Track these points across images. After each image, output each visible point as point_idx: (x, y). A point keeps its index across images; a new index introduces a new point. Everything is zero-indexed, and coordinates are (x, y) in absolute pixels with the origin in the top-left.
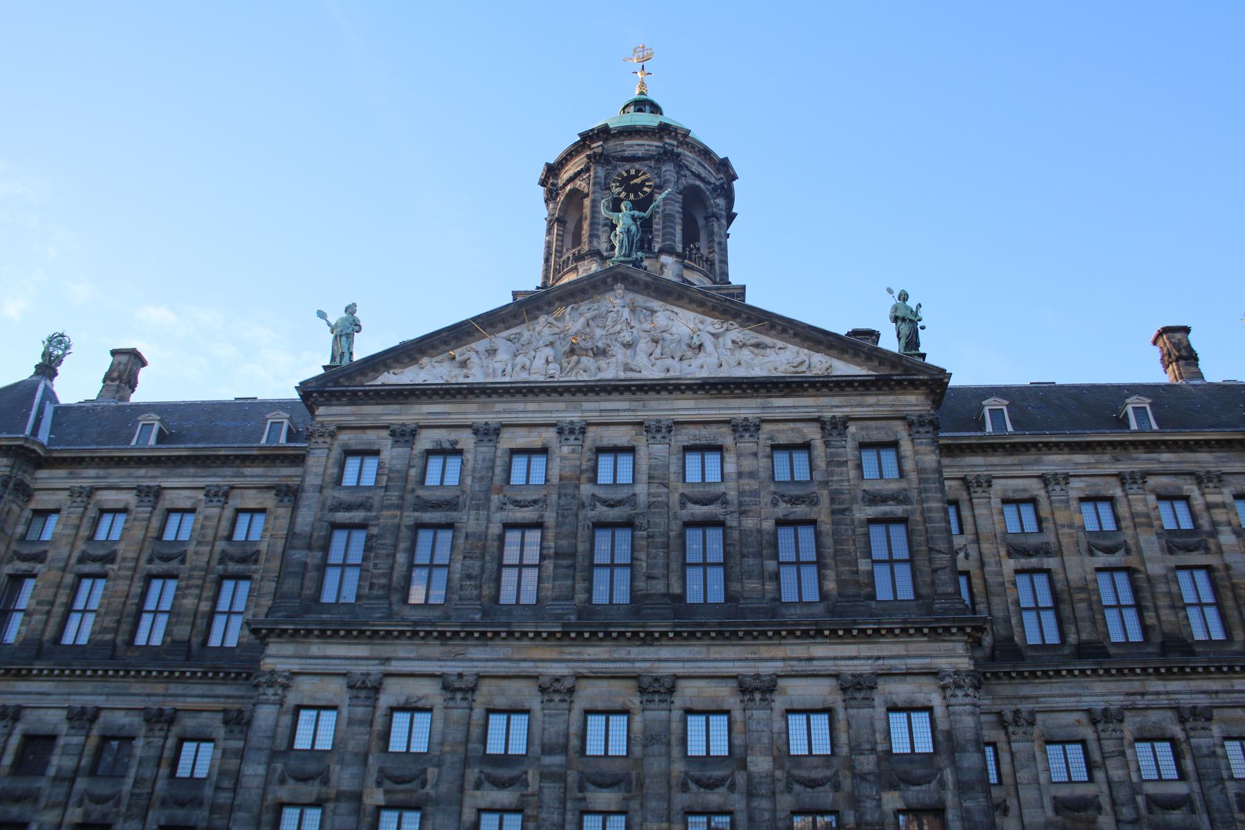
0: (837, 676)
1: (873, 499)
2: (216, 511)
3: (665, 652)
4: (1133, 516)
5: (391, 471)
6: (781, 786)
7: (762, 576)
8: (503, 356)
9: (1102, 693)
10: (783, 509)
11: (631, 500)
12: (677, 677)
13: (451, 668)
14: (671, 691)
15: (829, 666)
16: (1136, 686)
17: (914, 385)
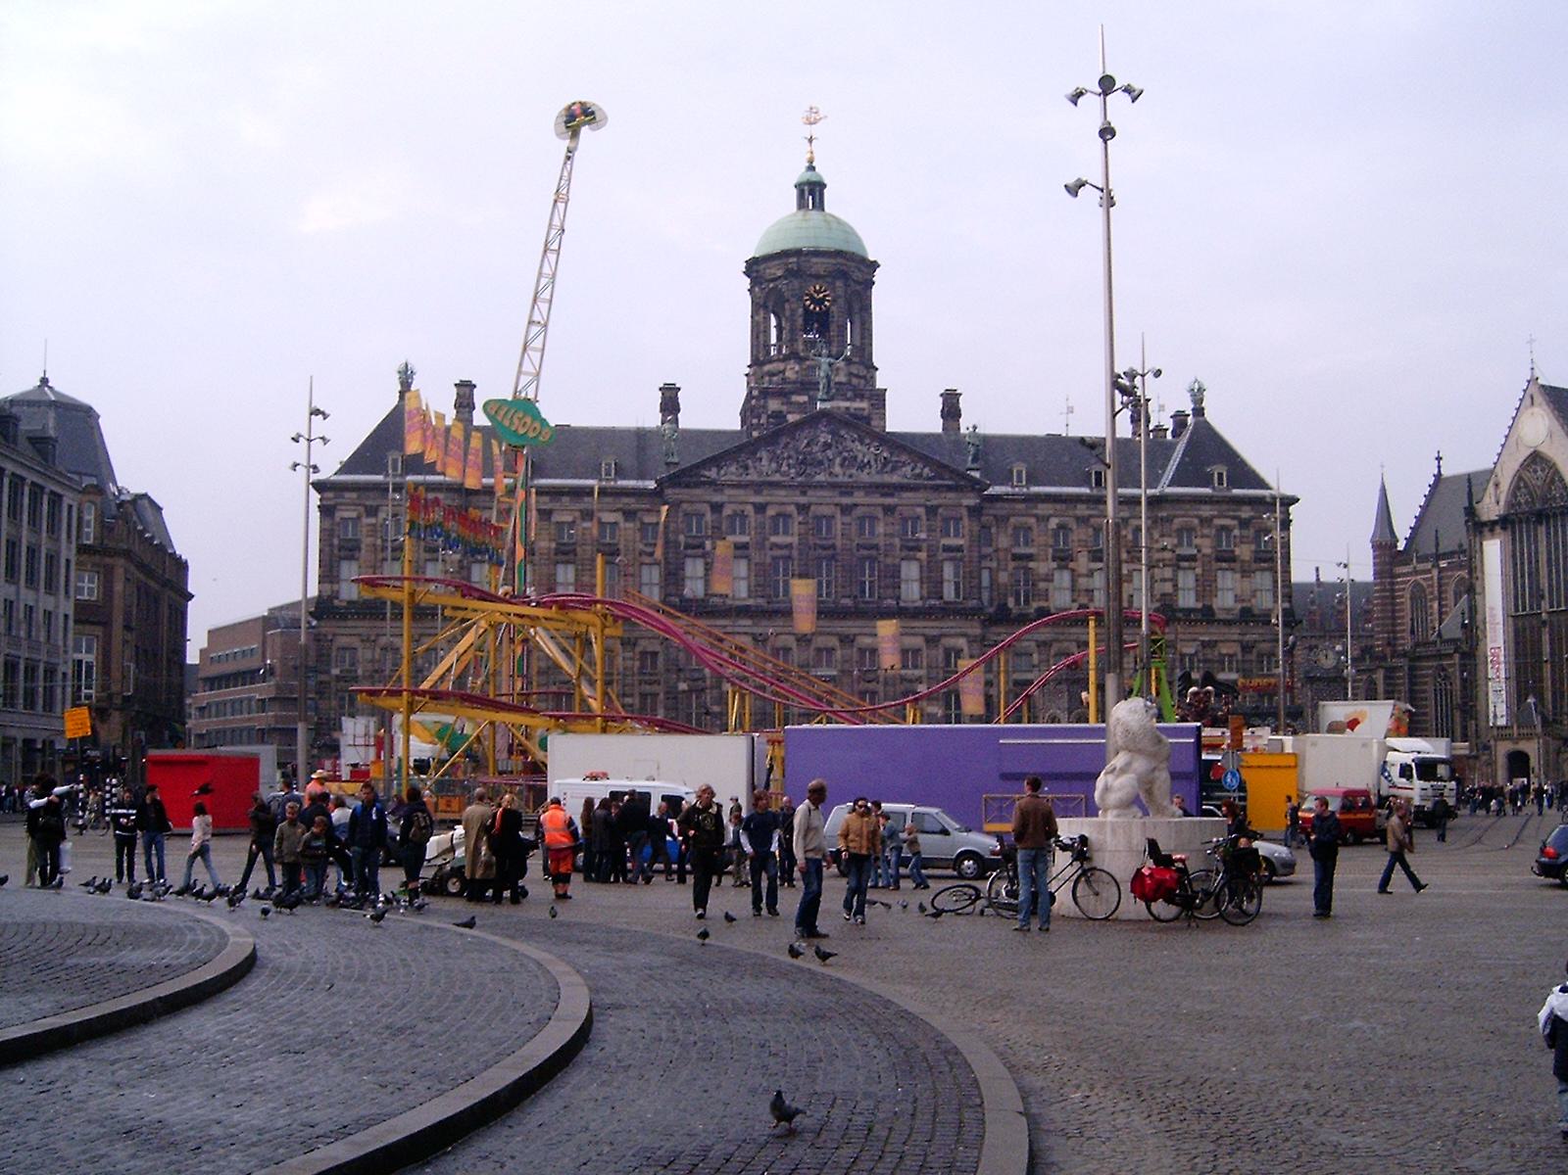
0: (924, 635)
1: (947, 549)
2: (587, 524)
3: (850, 623)
4: (1079, 541)
5: (713, 527)
6: (898, 681)
7: (894, 588)
8: (764, 462)
9: (1045, 634)
10: (904, 554)
11: (833, 547)
12: (855, 635)
13: (757, 630)
14: (853, 641)
15: (921, 631)
16: (1060, 630)
17: (973, 489)
